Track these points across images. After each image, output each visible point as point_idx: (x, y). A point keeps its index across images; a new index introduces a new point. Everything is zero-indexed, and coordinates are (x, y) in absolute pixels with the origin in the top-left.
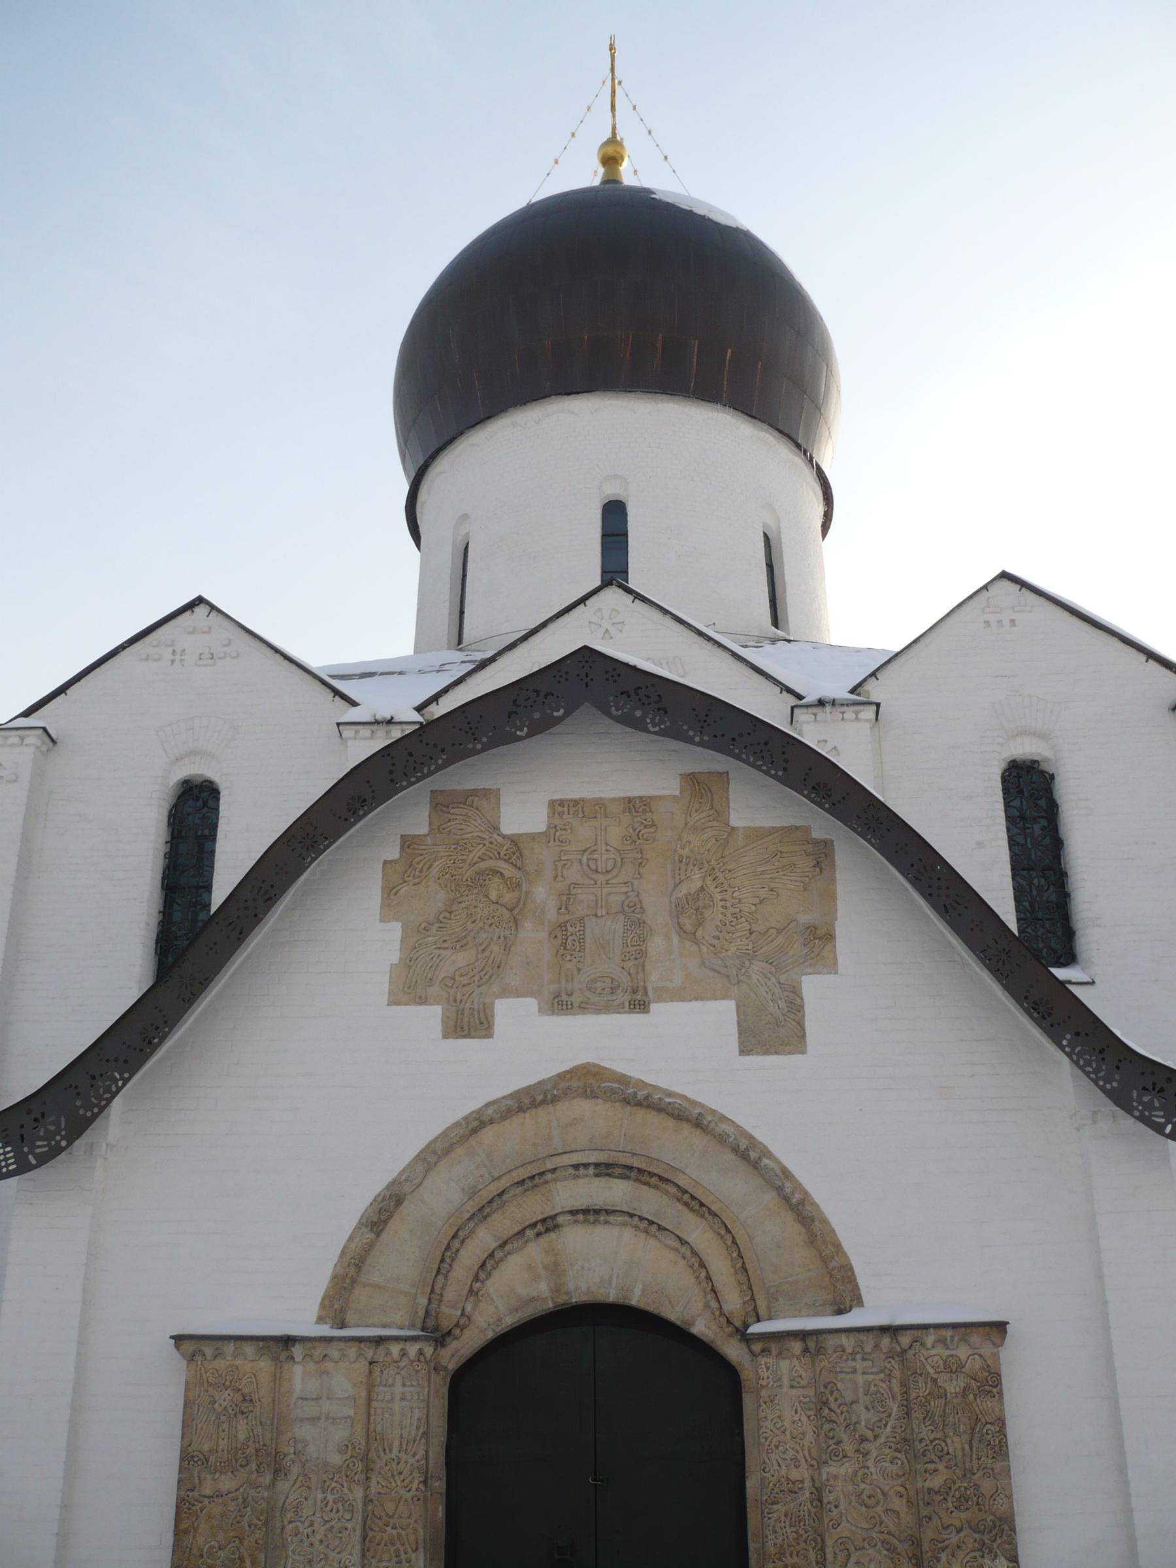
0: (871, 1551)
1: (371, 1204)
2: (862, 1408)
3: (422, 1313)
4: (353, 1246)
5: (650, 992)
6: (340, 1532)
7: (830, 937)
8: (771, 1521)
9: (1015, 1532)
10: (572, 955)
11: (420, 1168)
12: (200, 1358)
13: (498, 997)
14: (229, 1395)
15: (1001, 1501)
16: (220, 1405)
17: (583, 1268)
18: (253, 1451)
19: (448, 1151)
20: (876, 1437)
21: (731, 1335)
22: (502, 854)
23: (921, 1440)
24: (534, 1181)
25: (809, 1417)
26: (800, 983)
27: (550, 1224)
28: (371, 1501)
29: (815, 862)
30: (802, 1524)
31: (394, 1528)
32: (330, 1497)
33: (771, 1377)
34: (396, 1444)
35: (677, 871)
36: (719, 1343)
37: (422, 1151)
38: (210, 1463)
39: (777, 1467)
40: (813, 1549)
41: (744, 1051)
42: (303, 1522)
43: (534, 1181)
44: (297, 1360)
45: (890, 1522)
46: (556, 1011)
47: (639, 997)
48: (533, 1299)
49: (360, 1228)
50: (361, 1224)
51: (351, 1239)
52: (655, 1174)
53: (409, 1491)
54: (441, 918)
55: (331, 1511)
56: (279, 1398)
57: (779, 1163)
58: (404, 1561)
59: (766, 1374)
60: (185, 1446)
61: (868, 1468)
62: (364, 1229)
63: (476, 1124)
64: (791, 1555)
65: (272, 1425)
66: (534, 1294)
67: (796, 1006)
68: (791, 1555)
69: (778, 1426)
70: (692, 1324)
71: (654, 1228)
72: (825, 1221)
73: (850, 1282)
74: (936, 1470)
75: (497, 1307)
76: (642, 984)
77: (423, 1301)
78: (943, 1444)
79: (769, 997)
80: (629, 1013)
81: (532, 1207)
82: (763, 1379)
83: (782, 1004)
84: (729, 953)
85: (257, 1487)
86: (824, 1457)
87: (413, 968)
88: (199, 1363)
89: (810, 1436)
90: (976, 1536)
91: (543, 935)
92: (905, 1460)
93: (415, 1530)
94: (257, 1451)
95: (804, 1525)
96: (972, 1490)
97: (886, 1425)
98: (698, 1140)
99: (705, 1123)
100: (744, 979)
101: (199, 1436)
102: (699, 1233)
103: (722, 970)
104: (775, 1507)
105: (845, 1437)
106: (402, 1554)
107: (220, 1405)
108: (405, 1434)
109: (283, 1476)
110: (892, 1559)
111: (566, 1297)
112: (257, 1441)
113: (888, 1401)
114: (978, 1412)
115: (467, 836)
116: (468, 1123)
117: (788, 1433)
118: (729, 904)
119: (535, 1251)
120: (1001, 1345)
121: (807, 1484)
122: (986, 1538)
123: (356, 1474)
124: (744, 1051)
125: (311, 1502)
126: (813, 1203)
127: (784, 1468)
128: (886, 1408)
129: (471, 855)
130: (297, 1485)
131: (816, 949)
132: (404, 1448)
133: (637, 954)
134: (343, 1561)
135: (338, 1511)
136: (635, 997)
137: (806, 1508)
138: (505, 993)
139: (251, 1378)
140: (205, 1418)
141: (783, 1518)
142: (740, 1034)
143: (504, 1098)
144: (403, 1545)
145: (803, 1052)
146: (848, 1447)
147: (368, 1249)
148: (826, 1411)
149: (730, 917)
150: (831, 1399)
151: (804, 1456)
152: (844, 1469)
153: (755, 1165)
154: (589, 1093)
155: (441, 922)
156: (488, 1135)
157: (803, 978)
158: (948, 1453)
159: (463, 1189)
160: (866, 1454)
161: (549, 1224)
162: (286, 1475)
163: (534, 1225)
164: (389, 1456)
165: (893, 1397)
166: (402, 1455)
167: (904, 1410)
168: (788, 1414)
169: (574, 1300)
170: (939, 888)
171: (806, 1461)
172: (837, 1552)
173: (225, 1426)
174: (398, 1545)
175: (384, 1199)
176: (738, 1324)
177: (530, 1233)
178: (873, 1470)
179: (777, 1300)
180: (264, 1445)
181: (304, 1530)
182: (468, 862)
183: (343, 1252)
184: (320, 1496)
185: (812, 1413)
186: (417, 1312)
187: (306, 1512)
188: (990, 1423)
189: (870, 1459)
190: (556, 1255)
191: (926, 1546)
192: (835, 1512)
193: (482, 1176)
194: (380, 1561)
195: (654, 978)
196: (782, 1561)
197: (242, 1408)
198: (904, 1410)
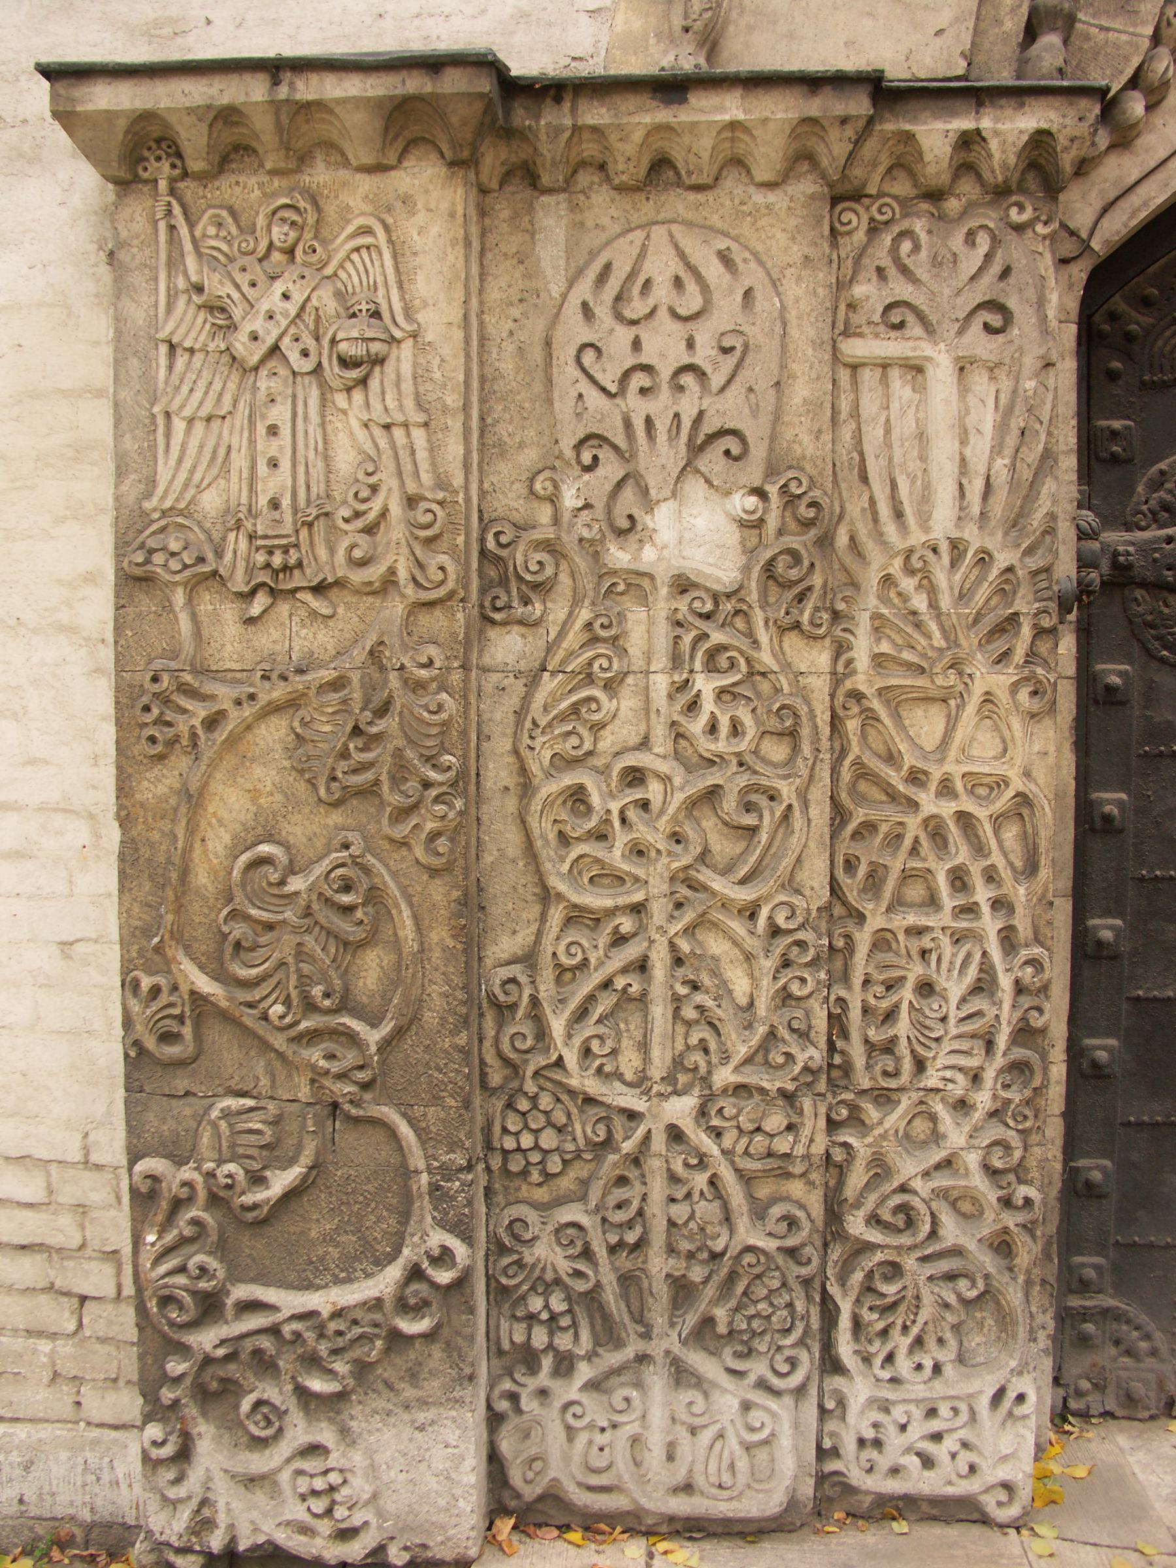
6: (749, 807)
12: (166, 166)
14: (286, 296)
16: (255, 337)
31: (946, 789)
32: (705, 685)
34: (945, 493)
38: (228, 556)
42: (604, 771)
44: (546, 180)
56: (482, 324)
58: (985, 909)
60: (130, 500)
65: (466, 407)
88: (163, 185)
101: (180, 461)
106: (978, 881)
107: (255, 337)
112: (408, 468)
123: (801, 598)
125: (628, 703)
132: (976, 510)
134: (764, 912)
139: (367, 231)
140: (198, 394)
164: (917, 538)
166: (973, 537)
173: (280, 414)
174: (962, 854)
197: (343, 347)
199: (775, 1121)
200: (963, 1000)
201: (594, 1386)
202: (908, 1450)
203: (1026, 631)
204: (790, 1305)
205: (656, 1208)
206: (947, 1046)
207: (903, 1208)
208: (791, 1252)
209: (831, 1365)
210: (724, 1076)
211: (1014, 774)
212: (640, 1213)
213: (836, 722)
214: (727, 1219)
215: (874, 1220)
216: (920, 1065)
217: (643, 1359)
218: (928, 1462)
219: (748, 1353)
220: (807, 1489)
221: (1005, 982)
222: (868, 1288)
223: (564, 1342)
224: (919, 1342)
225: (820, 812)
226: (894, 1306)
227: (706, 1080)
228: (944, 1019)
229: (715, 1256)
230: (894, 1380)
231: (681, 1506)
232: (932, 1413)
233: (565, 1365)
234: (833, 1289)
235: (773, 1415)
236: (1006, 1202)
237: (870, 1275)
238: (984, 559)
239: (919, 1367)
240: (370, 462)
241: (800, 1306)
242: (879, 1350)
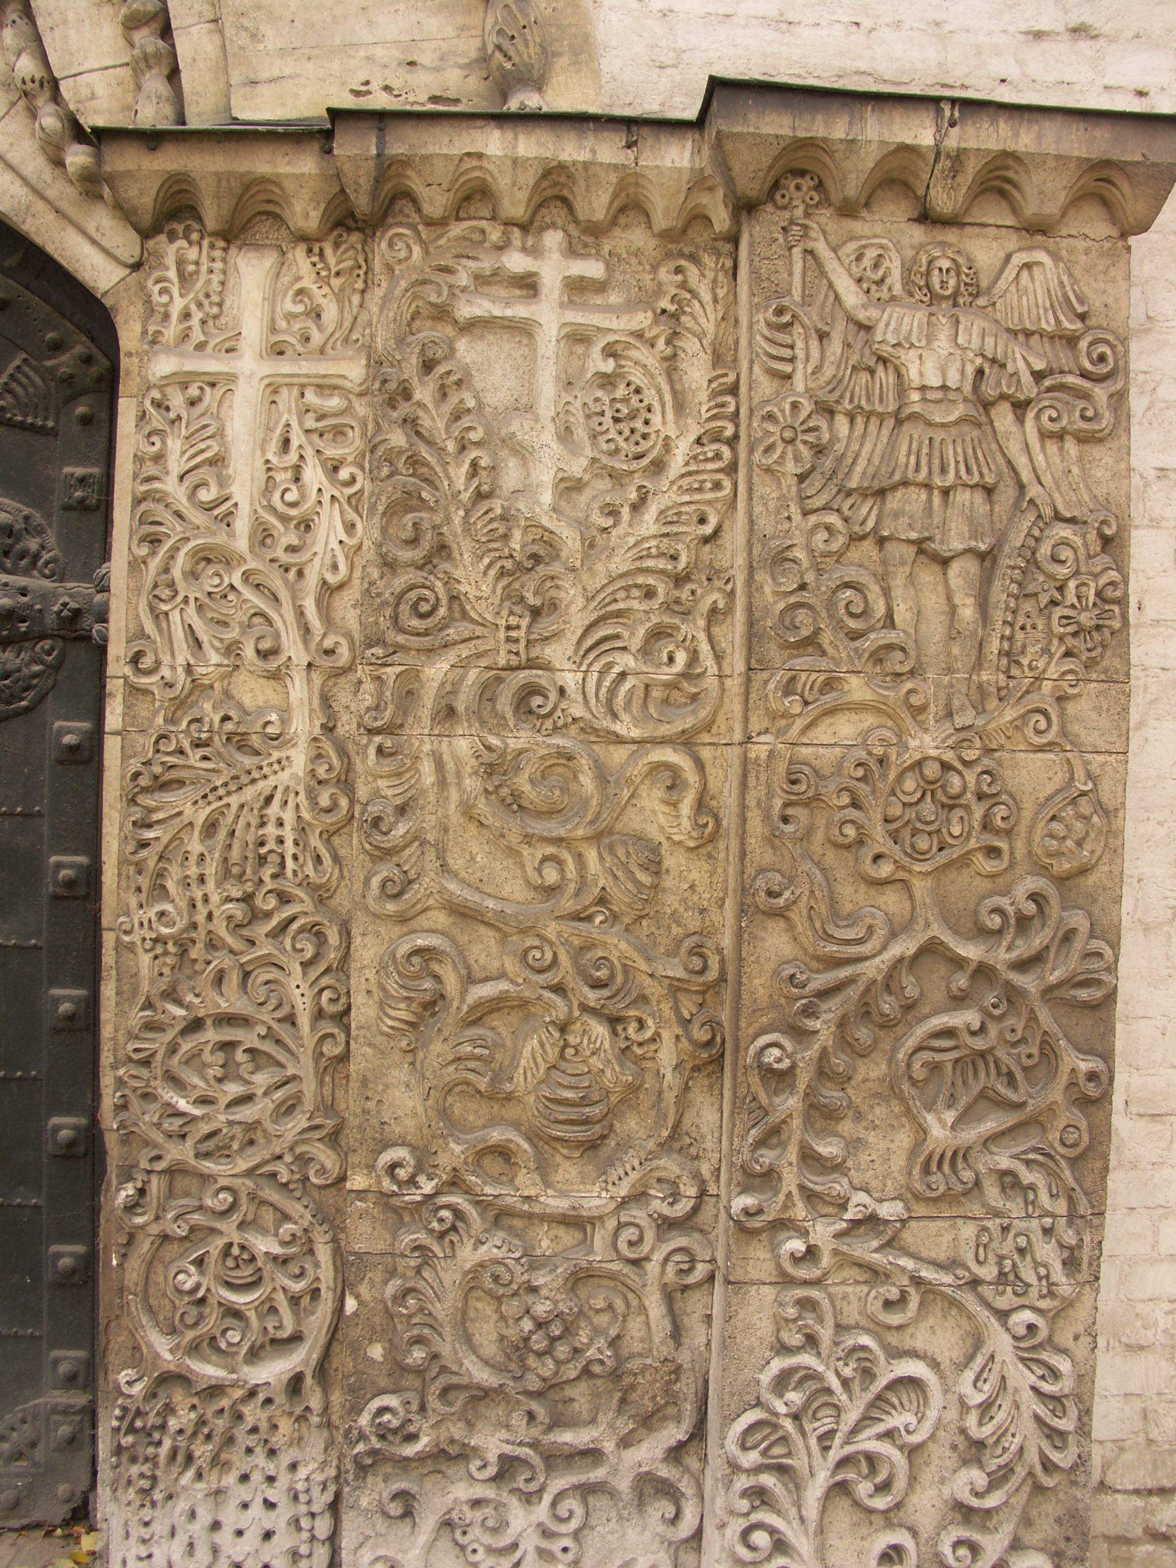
2: (548, 435)
9: (1115, 945)
15: (1079, 826)
30: (267, 873)
33: (197, 316)
39: (183, 655)
40: (306, 965)
61: (547, 667)
68: (219, 979)
69: (204, 495)
78: (874, 592)
82: (166, 316)
92: (704, 648)
95: (275, 876)
96: (971, 778)
113: (656, 419)
114: (1026, 475)
120: (1143, 227)
127: (215, 658)
128: (644, 445)
137: (289, 816)
141: (195, 846)
150: (424, 393)
151: (300, 613)
158: (889, 620)
165: (680, 407)
167: (718, 456)
171: (306, 630)
178: (570, 680)
188: (1072, 521)
189: (556, 635)
196: (179, 1003)
198: (718, 456)
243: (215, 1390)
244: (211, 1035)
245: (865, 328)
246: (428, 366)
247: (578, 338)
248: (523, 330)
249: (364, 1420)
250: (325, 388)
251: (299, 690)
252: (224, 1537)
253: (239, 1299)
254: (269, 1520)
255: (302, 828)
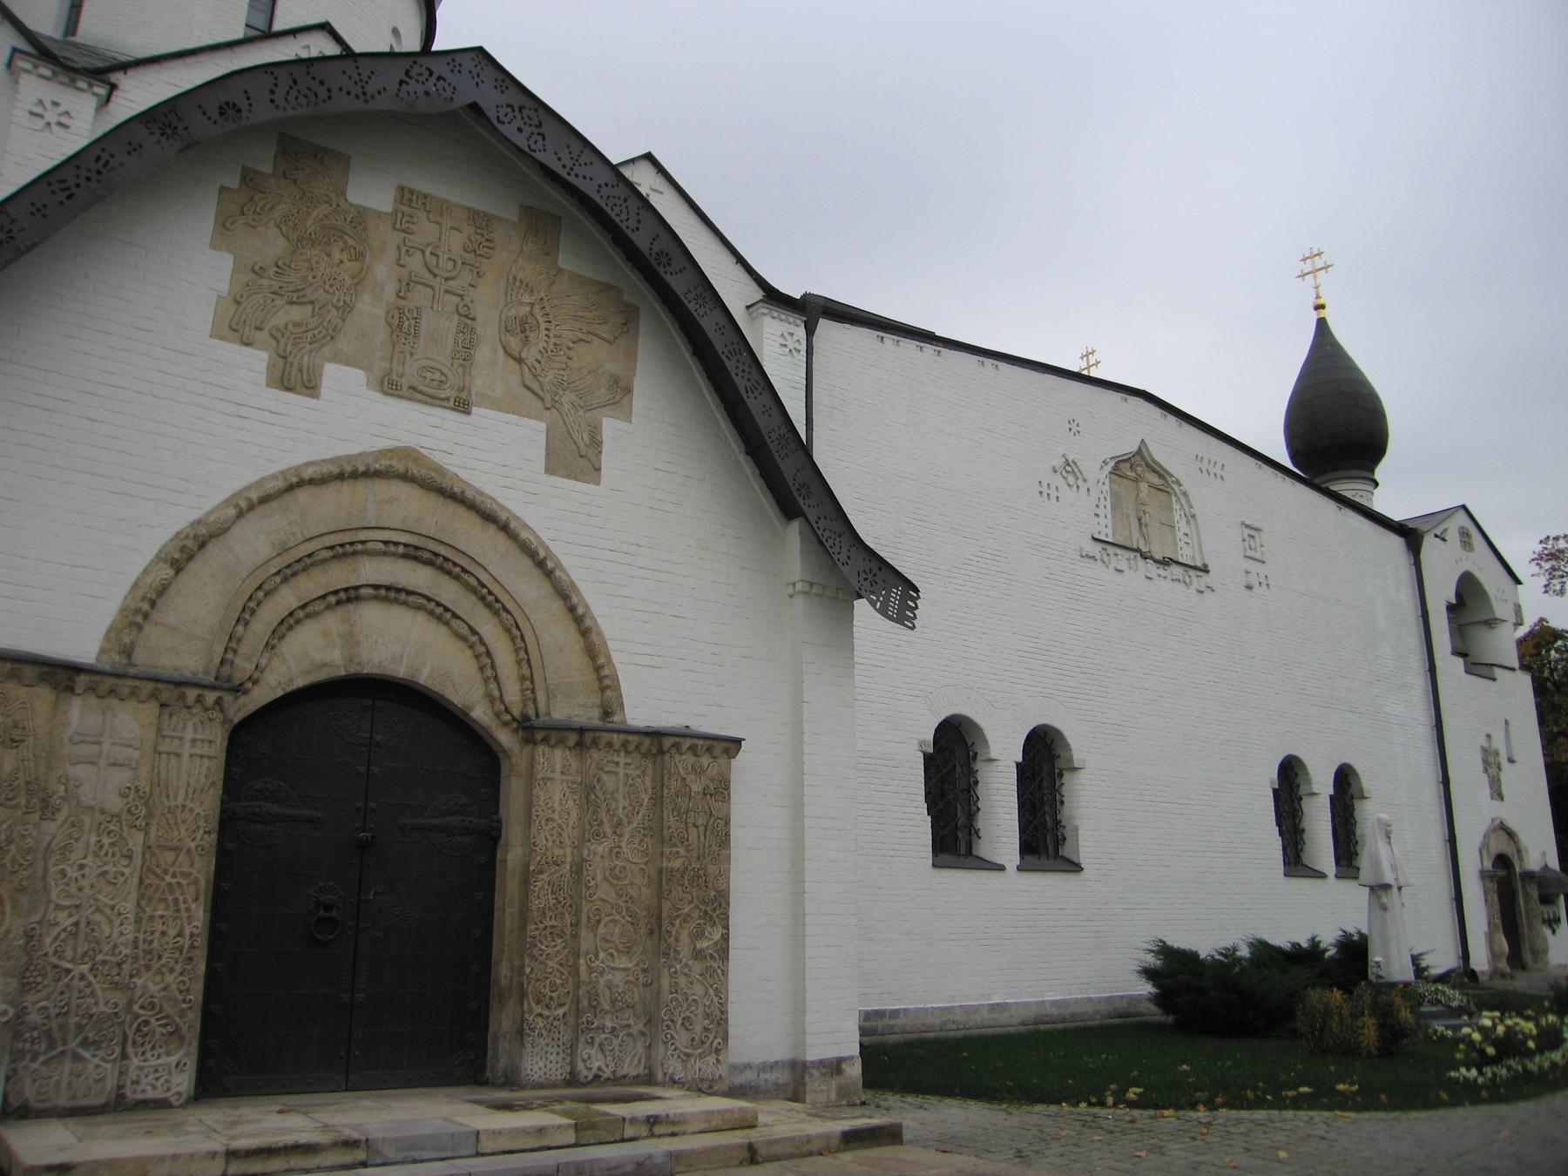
0: (617, 917)
1: (172, 540)
3: (217, 661)
4: (149, 580)
5: (473, 393)
7: (628, 391)
8: (536, 889)
10: (406, 339)
11: (232, 512)
13: (329, 361)
17: (377, 642)
18: (23, 784)
19: (264, 500)
20: (629, 823)
21: (506, 724)
22: (349, 220)
23: (669, 827)
24: (344, 552)
25: (575, 801)
26: (601, 422)
27: (353, 593)
28: (150, 847)
29: (624, 321)
31: (174, 875)
34: (182, 791)
35: (509, 293)
36: (493, 729)
37: (233, 496)
39: (545, 842)
41: (550, 470)
42: (72, 866)
43: (344, 552)
44: (77, 691)
45: (633, 892)
46: (386, 389)
47: (464, 397)
48: (325, 665)
49: (157, 563)
50: (159, 558)
51: (146, 572)
52: (460, 566)
53: (193, 840)
54: (280, 263)
55: (106, 854)
57: (568, 576)
59: (542, 760)
62: (161, 564)
63: (295, 480)
64: (551, 918)
66: (328, 660)
67: (596, 443)
68: (551, 918)
69: (550, 805)
70: (471, 709)
71: (448, 615)
72: (600, 634)
73: (615, 690)
74: (678, 853)
75: (289, 667)
76: (467, 385)
77: (220, 650)
79: (576, 427)
80: (452, 409)
81: (339, 575)
83: (585, 435)
84: (547, 379)
85: (25, 824)
86: (586, 835)
87: (244, 305)
89: (574, 815)
90: (703, 907)
91: (381, 313)
93: (196, 881)
94: (28, 783)
97: (638, 813)
98: (502, 542)
99: (512, 526)
100: (557, 405)
102: (489, 628)
103: (539, 392)
104: (541, 876)
105: (605, 821)
108: (193, 782)
109: (50, 815)
110: (633, 924)
111: (358, 668)
115: (316, 191)
116: (285, 479)
117: (557, 813)
118: (552, 335)
119: (332, 621)
121: (569, 859)
122: (709, 909)
123: (137, 819)
124: (550, 470)
125: (81, 844)
126: (593, 618)
129: (316, 211)
130: (66, 826)
131: (618, 397)
132: (190, 796)
133: (465, 353)
134: (117, 907)
135: (113, 855)
136: (460, 395)
138: (337, 358)
142: (547, 454)
143: (323, 461)
144: (183, 894)
145: (598, 484)
146: (609, 831)
147: (163, 590)
148: (593, 797)
149: (551, 346)
150: (598, 787)
152: (602, 848)
153: (549, 574)
154: (406, 478)
155: (278, 267)
156: (303, 495)
157: (604, 419)
159: (273, 544)
160: (621, 836)
161: (350, 596)
162: (53, 813)
163: (336, 592)
164: (173, 803)
168: (557, 797)
169: (365, 672)
170: (743, 371)
172: (592, 916)
175: (187, 537)
176: (516, 713)
177: (332, 599)
178: (625, 850)
179: (555, 697)
180: (36, 779)
181: (72, 873)
182: (313, 216)
183: (135, 586)
184: (93, 839)
185: (577, 797)
186: (212, 660)
187: (76, 856)
190: (353, 626)
191: (664, 915)
192: (593, 883)
193: (294, 534)
194: (155, 910)
195: (478, 383)
199: (115, 971)
200: (175, 938)
201: (45, 1063)
202: (147, 1084)
203: (201, 832)
204: (114, 1031)
205: (74, 1002)
206: (169, 951)
207: (151, 1003)
208: (116, 1014)
209: (124, 1056)
210: (100, 957)
211: (194, 872)
212: (67, 1004)
213: (144, 854)
214: (96, 1004)
215: (142, 1007)
216: (160, 957)
217: (63, 1052)
218: (154, 1088)
219: (99, 1048)
220: (113, 1097)
221: (187, 932)
222: (138, 1030)
223: (36, 1047)
224: (153, 1048)
225: (136, 880)
226: (147, 1034)
227: (93, 960)
228: (167, 943)
229: (91, 1016)
230: (145, 1061)
231: (72, 1104)
232: (156, 1071)
233: (35, 1057)
234: (127, 1030)
235: (105, 1069)
236: (184, 1001)
237: (139, 1025)
238: (191, 810)
239: (153, 1055)
240: (17, 770)
241: (117, 1032)
242: (140, 1050)
243: (548, 1017)
244: (549, 930)
245: (685, 779)
246: (598, 781)
247: (627, 775)
248: (616, 773)
249: (584, 1019)
250: (573, 783)
251: (569, 851)
252: (548, 1055)
253: (553, 994)
254: (558, 1050)
255: (568, 881)
